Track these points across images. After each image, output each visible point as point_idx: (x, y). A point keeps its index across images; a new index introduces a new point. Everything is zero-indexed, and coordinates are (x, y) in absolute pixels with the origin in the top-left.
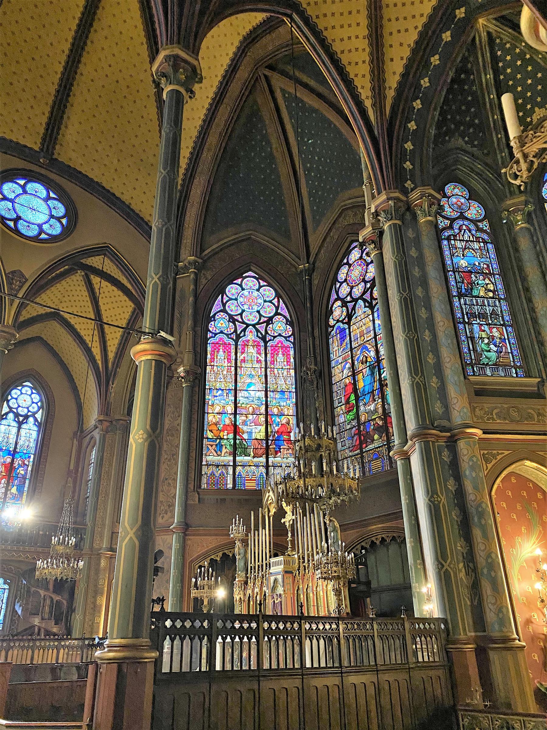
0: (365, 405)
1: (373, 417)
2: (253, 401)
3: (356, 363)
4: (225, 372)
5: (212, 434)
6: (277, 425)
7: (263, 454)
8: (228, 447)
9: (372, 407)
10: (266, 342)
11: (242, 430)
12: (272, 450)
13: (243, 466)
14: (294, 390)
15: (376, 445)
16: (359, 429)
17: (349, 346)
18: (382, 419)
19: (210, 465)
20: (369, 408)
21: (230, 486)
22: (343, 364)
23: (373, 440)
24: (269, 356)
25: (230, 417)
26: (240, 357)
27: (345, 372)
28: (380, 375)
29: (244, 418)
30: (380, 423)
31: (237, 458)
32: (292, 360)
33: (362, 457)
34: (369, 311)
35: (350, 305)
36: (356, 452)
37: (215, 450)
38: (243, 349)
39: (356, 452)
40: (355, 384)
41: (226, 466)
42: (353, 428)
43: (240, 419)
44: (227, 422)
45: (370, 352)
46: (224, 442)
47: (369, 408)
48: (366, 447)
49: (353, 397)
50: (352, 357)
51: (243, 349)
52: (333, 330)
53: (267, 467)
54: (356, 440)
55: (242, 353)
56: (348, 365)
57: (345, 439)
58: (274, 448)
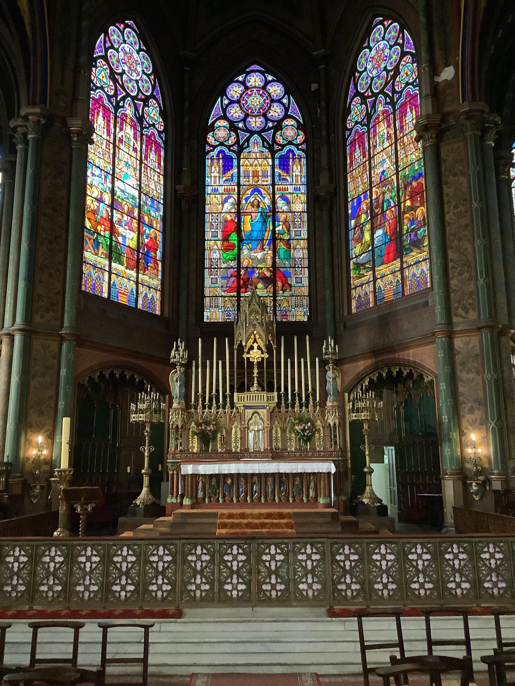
0: (250, 250)
1: (259, 266)
2: (128, 198)
3: (243, 202)
4: (104, 147)
5: (90, 225)
6: (147, 237)
7: (134, 268)
8: (105, 246)
9: (259, 255)
10: (142, 129)
11: (118, 230)
12: (142, 265)
13: (117, 275)
14: (162, 202)
16: (239, 271)
17: (235, 179)
18: (270, 271)
19: (88, 263)
20: (255, 255)
21: (105, 295)
24: (144, 146)
25: (108, 209)
26: (119, 135)
27: (226, 205)
28: (274, 227)
29: (119, 216)
30: (268, 274)
31: (114, 265)
32: (162, 164)
33: (239, 301)
36: (232, 294)
37: (92, 246)
38: (122, 124)
39: (232, 294)
42: (230, 268)
43: (117, 216)
44: (105, 215)
45: (264, 198)
46: (101, 239)
47: (255, 255)
48: (246, 292)
49: (234, 237)
50: (239, 193)
51: (122, 124)
52: (213, 150)
53: (137, 283)
54: (233, 282)
55: (121, 129)
57: (216, 277)
58: (143, 263)
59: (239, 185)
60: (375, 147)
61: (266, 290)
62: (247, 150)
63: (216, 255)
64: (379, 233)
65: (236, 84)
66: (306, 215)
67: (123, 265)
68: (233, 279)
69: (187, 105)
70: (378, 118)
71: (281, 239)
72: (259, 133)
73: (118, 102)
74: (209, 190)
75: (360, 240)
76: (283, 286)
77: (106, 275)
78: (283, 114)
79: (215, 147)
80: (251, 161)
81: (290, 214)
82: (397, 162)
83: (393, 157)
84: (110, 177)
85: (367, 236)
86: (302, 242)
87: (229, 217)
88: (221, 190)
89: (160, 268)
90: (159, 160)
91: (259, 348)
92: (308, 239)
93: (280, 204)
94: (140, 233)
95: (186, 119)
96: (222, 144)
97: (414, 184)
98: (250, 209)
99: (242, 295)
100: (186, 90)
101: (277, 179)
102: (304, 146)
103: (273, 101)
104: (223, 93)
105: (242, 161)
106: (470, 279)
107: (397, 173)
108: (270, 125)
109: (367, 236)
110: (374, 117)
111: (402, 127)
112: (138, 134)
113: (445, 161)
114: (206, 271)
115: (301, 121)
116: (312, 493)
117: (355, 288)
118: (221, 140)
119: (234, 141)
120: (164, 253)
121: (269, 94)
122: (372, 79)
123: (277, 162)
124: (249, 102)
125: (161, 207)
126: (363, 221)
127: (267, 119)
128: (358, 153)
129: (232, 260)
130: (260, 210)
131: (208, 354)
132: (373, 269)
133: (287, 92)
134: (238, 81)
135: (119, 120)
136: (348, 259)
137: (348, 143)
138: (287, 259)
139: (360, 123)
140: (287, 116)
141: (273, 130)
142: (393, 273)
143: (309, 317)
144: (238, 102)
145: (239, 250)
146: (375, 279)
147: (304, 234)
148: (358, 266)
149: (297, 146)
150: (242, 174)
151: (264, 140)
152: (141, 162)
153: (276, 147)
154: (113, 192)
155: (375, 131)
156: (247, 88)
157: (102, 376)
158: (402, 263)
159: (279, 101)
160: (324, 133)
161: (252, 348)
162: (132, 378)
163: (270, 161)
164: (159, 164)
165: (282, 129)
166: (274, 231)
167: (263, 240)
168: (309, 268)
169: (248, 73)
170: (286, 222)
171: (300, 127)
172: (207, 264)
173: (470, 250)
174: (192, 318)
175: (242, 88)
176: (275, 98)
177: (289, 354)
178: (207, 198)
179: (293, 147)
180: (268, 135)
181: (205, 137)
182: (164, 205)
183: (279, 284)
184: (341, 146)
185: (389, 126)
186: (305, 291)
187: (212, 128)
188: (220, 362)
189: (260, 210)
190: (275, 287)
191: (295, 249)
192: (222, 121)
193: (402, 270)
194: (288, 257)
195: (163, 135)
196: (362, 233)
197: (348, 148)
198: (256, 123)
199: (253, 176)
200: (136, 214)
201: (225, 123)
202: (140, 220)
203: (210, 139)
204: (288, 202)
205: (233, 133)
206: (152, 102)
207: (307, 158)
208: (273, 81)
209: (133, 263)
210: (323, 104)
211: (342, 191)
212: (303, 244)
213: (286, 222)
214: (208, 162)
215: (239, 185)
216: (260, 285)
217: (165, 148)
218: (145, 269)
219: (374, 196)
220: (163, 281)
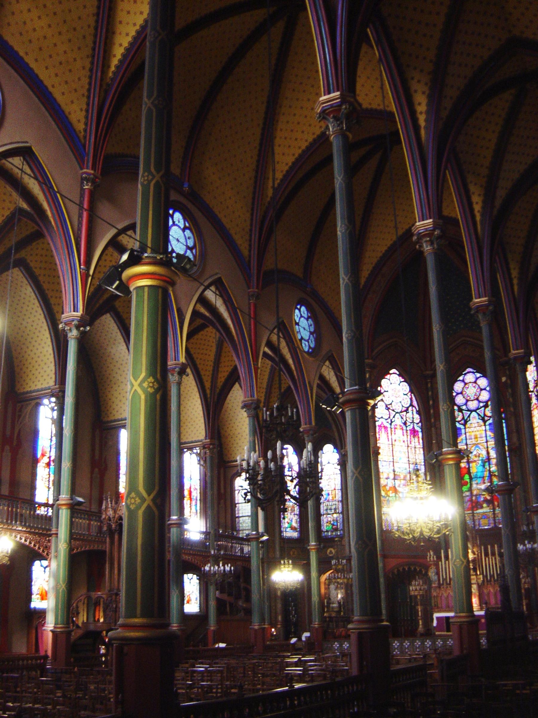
0: (477, 484)
10: (406, 427)
23: (482, 507)
28: (490, 468)
33: (473, 516)
36: (469, 512)
39: (469, 512)
48: (477, 510)
49: (467, 477)
61: (488, 508)
69: (431, 402)
71: (495, 475)
73: (391, 420)
84: (392, 463)
98: (476, 459)
103: (481, 390)
105: (467, 430)
108: (481, 405)
112: (405, 431)
121: (479, 385)
123: (488, 427)
127: (480, 402)
134: (460, 380)
135: (393, 430)
141: (483, 408)
145: (471, 485)
150: (468, 438)
151: (479, 415)
152: (408, 446)
153: (486, 418)
154: (394, 471)
156: (466, 384)
157: (398, 570)
160: (512, 409)
163: (483, 428)
166: (489, 471)
167: (483, 477)
169: (465, 374)
180: (481, 411)
182: (425, 465)
183: (496, 503)
189: (480, 459)
190: (493, 505)
198: (473, 405)
205: (460, 413)
208: (480, 377)
216: (485, 505)
217: (422, 432)
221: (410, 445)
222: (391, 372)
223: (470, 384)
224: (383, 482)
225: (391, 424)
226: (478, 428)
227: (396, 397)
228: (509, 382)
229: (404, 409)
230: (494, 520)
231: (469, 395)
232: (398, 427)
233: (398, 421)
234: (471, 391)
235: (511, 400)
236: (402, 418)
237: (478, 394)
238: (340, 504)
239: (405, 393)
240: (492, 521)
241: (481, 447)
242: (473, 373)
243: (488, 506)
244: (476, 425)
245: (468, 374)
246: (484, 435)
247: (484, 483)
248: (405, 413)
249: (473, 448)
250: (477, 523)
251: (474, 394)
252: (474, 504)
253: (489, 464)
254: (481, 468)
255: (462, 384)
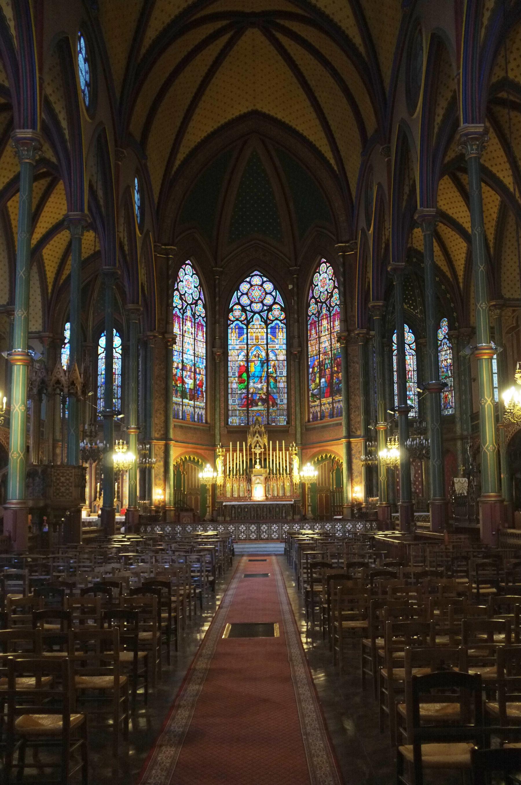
0: (254, 383)
1: (259, 392)
3: (250, 354)
9: (259, 386)
10: (195, 319)
13: (186, 406)
14: (205, 358)
15: (259, 408)
17: (245, 341)
18: (265, 395)
22: (239, 351)
23: (257, 405)
27: (240, 356)
28: (268, 369)
30: (264, 397)
33: (248, 413)
34: (263, 325)
35: (250, 315)
36: (244, 409)
39: (244, 409)
40: (247, 367)
41: (179, 404)
46: (178, 388)
48: (252, 407)
49: (245, 375)
52: (232, 324)
53: (194, 407)
56: (243, 353)
59: (247, 344)
60: (321, 332)
62: (252, 323)
63: (235, 386)
64: (323, 380)
65: (245, 283)
66: (286, 362)
67: (187, 399)
68: (244, 400)
69: (217, 299)
70: (323, 316)
71: (272, 377)
72: (259, 313)
73: (184, 311)
74: (230, 347)
75: (314, 381)
76: (273, 404)
77: (181, 406)
78: (273, 301)
79: (233, 321)
80: (254, 330)
81: (276, 362)
82: (331, 345)
83: (330, 341)
84: (181, 354)
85: (317, 380)
86: (283, 378)
87: (242, 364)
88: (237, 347)
89: (205, 396)
90: (203, 334)
91: (260, 446)
92: (287, 376)
93: (271, 356)
94: (195, 379)
95: (217, 308)
96: (237, 320)
97: (338, 359)
98: (254, 359)
99: (250, 409)
100: (217, 290)
101: (269, 341)
102: (285, 321)
103: (267, 294)
104: (238, 289)
105: (249, 330)
106: (359, 415)
107: (331, 351)
108: (265, 308)
109: (317, 380)
110: (321, 315)
111: (333, 327)
112: (193, 324)
113: (350, 354)
114: (230, 395)
115: (283, 306)
116: (284, 515)
117: (312, 407)
118: (237, 317)
119: (245, 318)
120: (206, 387)
121: (265, 289)
122: (321, 292)
123: (269, 330)
124: (253, 294)
125: (204, 361)
126: (315, 371)
127: (264, 305)
128: (313, 332)
129: (244, 389)
130: (260, 359)
131: (235, 450)
132: (320, 399)
133: (275, 288)
134: (246, 281)
135: (184, 320)
136: (309, 390)
137: (309, 323)
138: (275, 388)
139: (315, 314)
140: (275, 303)
142: (329, 403)
143: (287, 423)
144: (247, 294)
145: (248, 383)
146: (321, 405)
147: (285, 374)
148: (313, 395)
149: (281, 321)
150: (249, 338)
151: (261, 317)
152: (195, 339)
153: (268, 321)
155: (321, 323)
156: (252, 286)
158: (333, 399)
159: (270, 293)
160: (296, 316)
161: (256, 446)
162: (194, 458)
163: (265, 330)
164: (203, 337)
165: (272, 311)
166: (267, 372)
167: (261, 377)
168: (288, 393)
169: (252, 276)
170: (274, 366)
171: (282, 309)
172: (230, 391)
173: (359, 401)
174: (223, 424)
175: (249, 286)
176: (268, 291)
177: (274, 449)
178: (229, 351)
179: (278, 322)
181: (228, 316)
182: (206, 359)
183: (271, 403)
184: (305, 325)
185: (328, 323)
186: (285, 407)
187: (232, 310)
188: (241, 454)
189: (260, 359)
190: (268, 404)
191: (279, 382)
192: (237, 306)
193: (332, 403)
194: (276, 387)
195: (205, 319)
196: (315, 378)
197: (309, 326)
198: (257, 307)
199: (256, 339)
200: (193, 370)
201: (239, 307)
202: (195, 372)
203: (231, 317)
204: (276, 355)
205: (244, 313)
206: (200, 302)
207: (286, 328)
209: (192, 397)
210: (296, 298)
211: (305, 354)
212: (284, 379)
213: (274, 366)
214: (230, 331)
215: (247, 344)
216: (260, 404)
217: (206, 326)
218: (198, 398)
219: (321, 360)
220: (206, 403)
221: (196, 338)
222: (187, 262)
223: (256, 287)
224: (175, 371)
225: (183, 315)
226: (260, 330)
227: (188, 288)
228: (295, 289)
229: (194, 301)
230: (268, 418)
231: (254, 297)
232: (188, 319)
233: (189, 313)
234: (256, 293)
235: (296, 307)
236: (192, 311)
237: (263, 297)
238: (120, 389)
239: (196, 286)
240: (265, 419)
241: (261, 348)
242: (260, 276)
243: (263, 405)
244: (258, 326)
245: (255, 277)
246: (265, 337)
247: (261, 383)
248: (194, 305)
249: (253, 349)
250: (251, 419)
251: (258, 297)
252: (249, 402)
253: (268, 366)
254: (259, 369)
255: (248, 286)
